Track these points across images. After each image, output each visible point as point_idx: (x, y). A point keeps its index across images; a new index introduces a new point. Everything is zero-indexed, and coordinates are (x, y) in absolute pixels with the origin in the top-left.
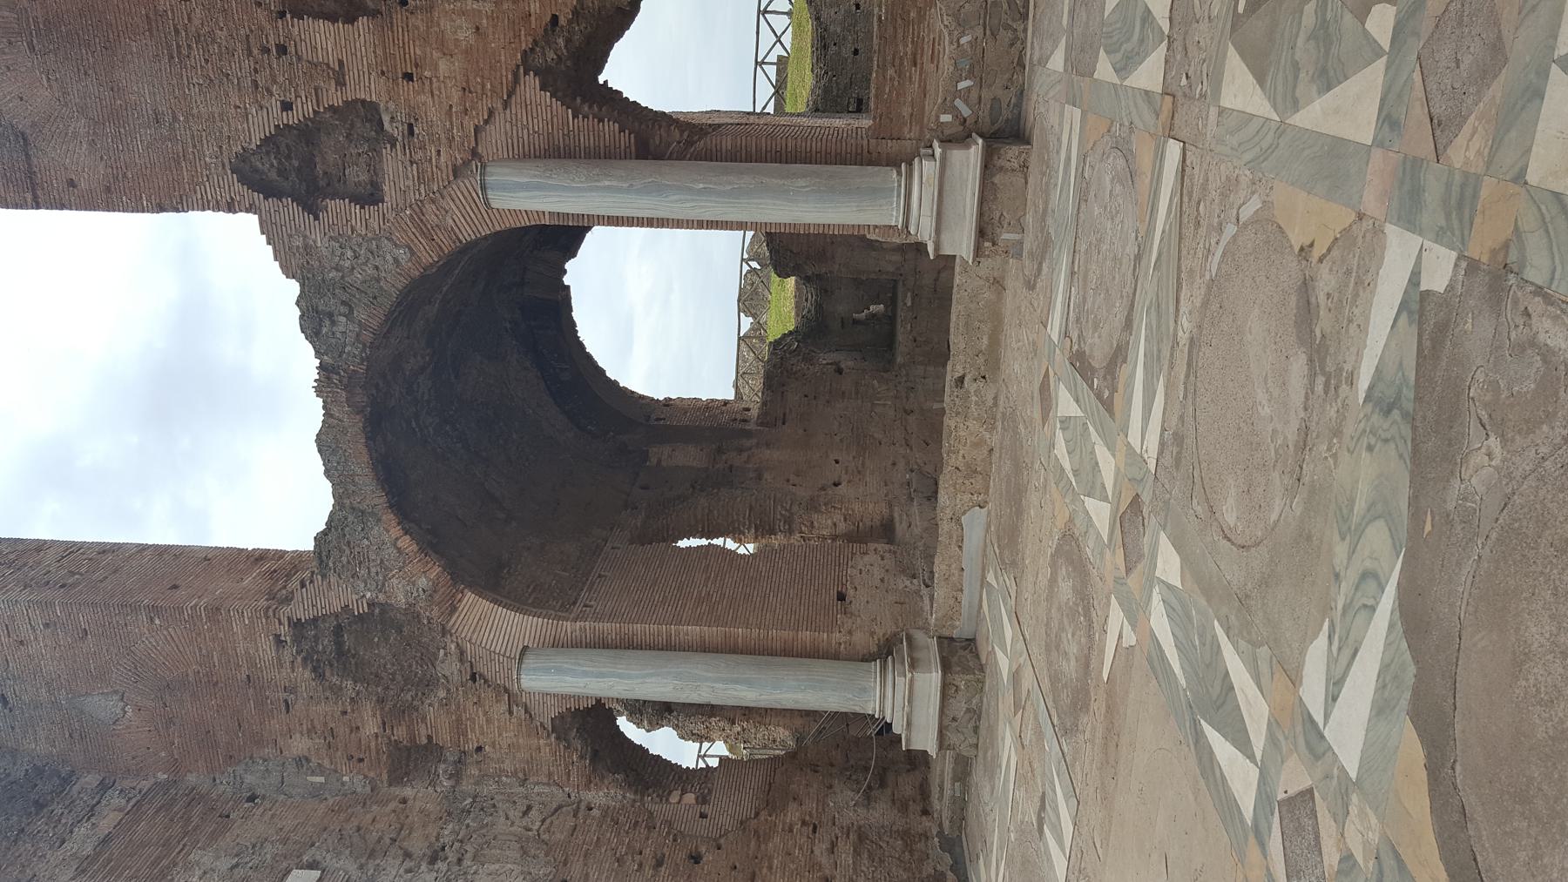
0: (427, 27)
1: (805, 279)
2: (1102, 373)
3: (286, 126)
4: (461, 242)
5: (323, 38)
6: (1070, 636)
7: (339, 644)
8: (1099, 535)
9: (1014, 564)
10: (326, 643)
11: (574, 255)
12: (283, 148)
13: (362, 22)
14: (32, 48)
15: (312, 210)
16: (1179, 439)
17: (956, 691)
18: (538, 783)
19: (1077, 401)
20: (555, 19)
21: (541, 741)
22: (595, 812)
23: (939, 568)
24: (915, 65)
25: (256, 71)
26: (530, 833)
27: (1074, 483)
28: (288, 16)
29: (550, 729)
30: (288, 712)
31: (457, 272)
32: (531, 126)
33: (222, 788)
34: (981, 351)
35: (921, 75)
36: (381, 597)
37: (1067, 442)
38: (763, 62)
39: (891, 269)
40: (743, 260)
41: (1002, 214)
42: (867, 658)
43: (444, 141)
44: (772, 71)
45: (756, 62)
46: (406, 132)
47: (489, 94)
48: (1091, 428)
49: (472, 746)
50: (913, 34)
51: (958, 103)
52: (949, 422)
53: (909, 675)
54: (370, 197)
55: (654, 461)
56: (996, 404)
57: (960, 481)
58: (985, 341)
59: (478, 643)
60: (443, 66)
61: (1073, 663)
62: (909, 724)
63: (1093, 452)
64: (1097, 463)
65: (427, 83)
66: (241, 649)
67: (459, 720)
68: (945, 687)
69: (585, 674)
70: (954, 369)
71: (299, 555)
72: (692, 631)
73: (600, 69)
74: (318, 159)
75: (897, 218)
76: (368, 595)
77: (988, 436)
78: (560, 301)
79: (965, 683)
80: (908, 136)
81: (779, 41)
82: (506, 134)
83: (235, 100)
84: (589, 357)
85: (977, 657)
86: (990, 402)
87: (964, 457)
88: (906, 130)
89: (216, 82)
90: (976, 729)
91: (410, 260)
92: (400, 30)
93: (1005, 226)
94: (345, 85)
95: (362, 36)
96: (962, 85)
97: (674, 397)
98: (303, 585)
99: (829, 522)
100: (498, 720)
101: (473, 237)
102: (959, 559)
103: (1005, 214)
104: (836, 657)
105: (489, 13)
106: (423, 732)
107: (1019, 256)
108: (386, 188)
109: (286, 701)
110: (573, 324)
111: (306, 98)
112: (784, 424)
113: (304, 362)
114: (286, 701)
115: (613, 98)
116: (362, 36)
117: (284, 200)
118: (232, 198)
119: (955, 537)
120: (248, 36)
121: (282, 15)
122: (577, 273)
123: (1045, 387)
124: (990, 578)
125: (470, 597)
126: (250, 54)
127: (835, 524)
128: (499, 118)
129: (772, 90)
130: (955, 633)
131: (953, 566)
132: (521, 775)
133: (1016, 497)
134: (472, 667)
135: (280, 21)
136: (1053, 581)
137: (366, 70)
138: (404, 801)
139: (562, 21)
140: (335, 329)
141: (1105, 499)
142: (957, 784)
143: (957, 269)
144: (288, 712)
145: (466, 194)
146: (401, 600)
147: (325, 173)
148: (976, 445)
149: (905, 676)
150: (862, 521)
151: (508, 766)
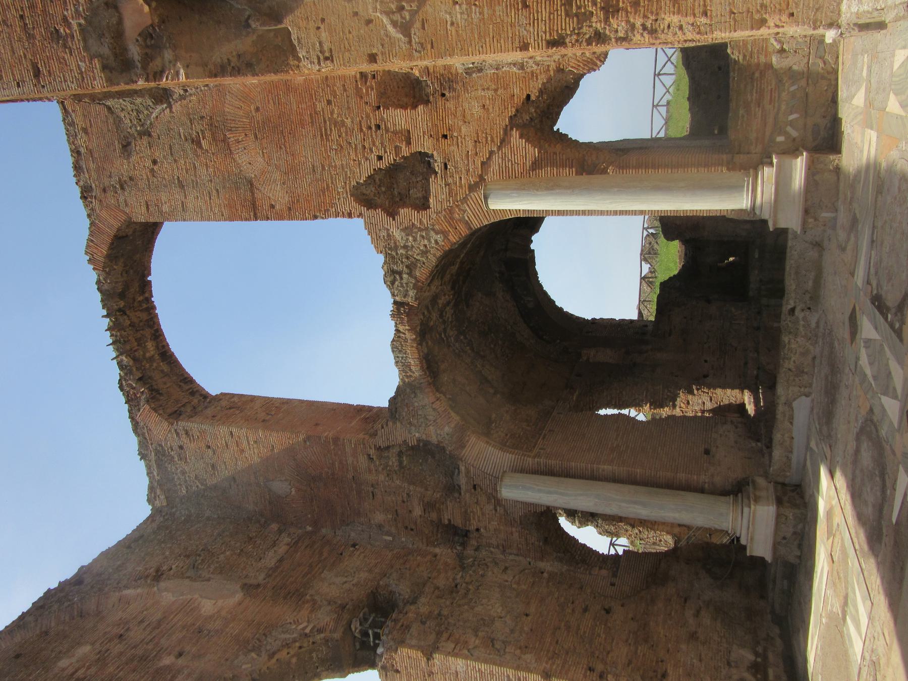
0: (456, 107)
1: (685, 242)
2: (893, 311)
3: (380, 169)
4: (471, 229)
5: (399, 118)
6: (869, 490)
7: (401, 462)
8: (891, 423)
9: (829, 436)
10: (393, 461)
11: (537, 231)
12: (377, 180)
13: (420, 108)
14: (256, 137)
15: (392, 214)
17: (786, 519)
18: (511, 554)
19: (876, 329)
20: (528, 96)
21: (514, 529)
22: (545, 575)
23: (777, 437)
24: (759, 106)
25: (364, 139)
26: (507, 583)
27: (873, 385)
28: (382, 109)
29: (519, 522)
30: (373, 499)
31: (469, 245)
32: (513, 160)
33: (339, 538)
35: (762, 112)
36: (424, 437)
37: (869, 356)
38: (657, 105)
40: (644, 228)
41: (821, 200)
42: (724, 493)
43: (464, 171)
44: (663, 110)
45: (653, 106)
46: (443, 168)
47: (490, 143)
48: (886, 349)
49: (473, 528)
50: (757, 86)
51: (789, 129)
52: (785, 339)
53: (752, 507)
54: (423, 205)
55: (585, 358)
56: (818, 326)
57: (792, 378)
58: (810, 283)
59: (477, 467)
60: (463, 129)
61: (870, 509)
62: (752, 539)
63: (887, 365)
64: (890, 373)
65: (455, 139)
66: (350, 461)
67: (466, 512)
68: (778, 516)
69: (540, 491)
70: (790, 302)
71: (380, 409)
72: (606, 468)
73: (555, 123)
74: (395, 186)
76: (417, 435)
78: (528, 259)
79: (793, 515)
80: (754, 152)
81: (668, 91)
82: (499, 164)
83: (353, 156)
84: (545, 293)
85: (802, 497)
86: (813, 325)
89: (344, 147)
90: (800, 546)
91: (443, 241)
92: (441, 111)
94: (410, 144)
95: (420, 116)
96: (791, 117)
97: (598, 318)
98: (382, 427)
99: (700, 401)
100: (488, 514)
101: (479, 226)
104: (701, 490)
105: (491, 97)
106: (446, 517)
107: (834, 228)
108: (431, 201)
109: (373, 493)
110: (536, 273)
111: (390, 153)
112: (670, 335)
113: (385, 301)
114: (373, 493)
115: (563, 138)
116: (420, 116)
117: (377, 210)
118: (351, 211)
119: (787, 416)
120: (360, 121)
121: (379, 108)
122: (539, 242)
123: (853, 318)
124: (813, 444)
125: (473, 439)
126: (361, 130)
127: (704, 403)
128: (496, 159)
129: (664, 122)
130: (787, 481)
131: (786, 435)
132: (501, 548)
133: (831, 390)
134: (473, 481)
135: (377, 112)
136: (857, 451)
137: (422, 134)
138: (435, 556)
139: (533, 98)
140: (402, 281)
141: (895, 397)
143: (790, 236)
144: (373, 499)
145: (475, 201)
146: (434, 440)
147: (399, 193)
148: (804, 354)
149: (750, 507)
151: (494, 541)
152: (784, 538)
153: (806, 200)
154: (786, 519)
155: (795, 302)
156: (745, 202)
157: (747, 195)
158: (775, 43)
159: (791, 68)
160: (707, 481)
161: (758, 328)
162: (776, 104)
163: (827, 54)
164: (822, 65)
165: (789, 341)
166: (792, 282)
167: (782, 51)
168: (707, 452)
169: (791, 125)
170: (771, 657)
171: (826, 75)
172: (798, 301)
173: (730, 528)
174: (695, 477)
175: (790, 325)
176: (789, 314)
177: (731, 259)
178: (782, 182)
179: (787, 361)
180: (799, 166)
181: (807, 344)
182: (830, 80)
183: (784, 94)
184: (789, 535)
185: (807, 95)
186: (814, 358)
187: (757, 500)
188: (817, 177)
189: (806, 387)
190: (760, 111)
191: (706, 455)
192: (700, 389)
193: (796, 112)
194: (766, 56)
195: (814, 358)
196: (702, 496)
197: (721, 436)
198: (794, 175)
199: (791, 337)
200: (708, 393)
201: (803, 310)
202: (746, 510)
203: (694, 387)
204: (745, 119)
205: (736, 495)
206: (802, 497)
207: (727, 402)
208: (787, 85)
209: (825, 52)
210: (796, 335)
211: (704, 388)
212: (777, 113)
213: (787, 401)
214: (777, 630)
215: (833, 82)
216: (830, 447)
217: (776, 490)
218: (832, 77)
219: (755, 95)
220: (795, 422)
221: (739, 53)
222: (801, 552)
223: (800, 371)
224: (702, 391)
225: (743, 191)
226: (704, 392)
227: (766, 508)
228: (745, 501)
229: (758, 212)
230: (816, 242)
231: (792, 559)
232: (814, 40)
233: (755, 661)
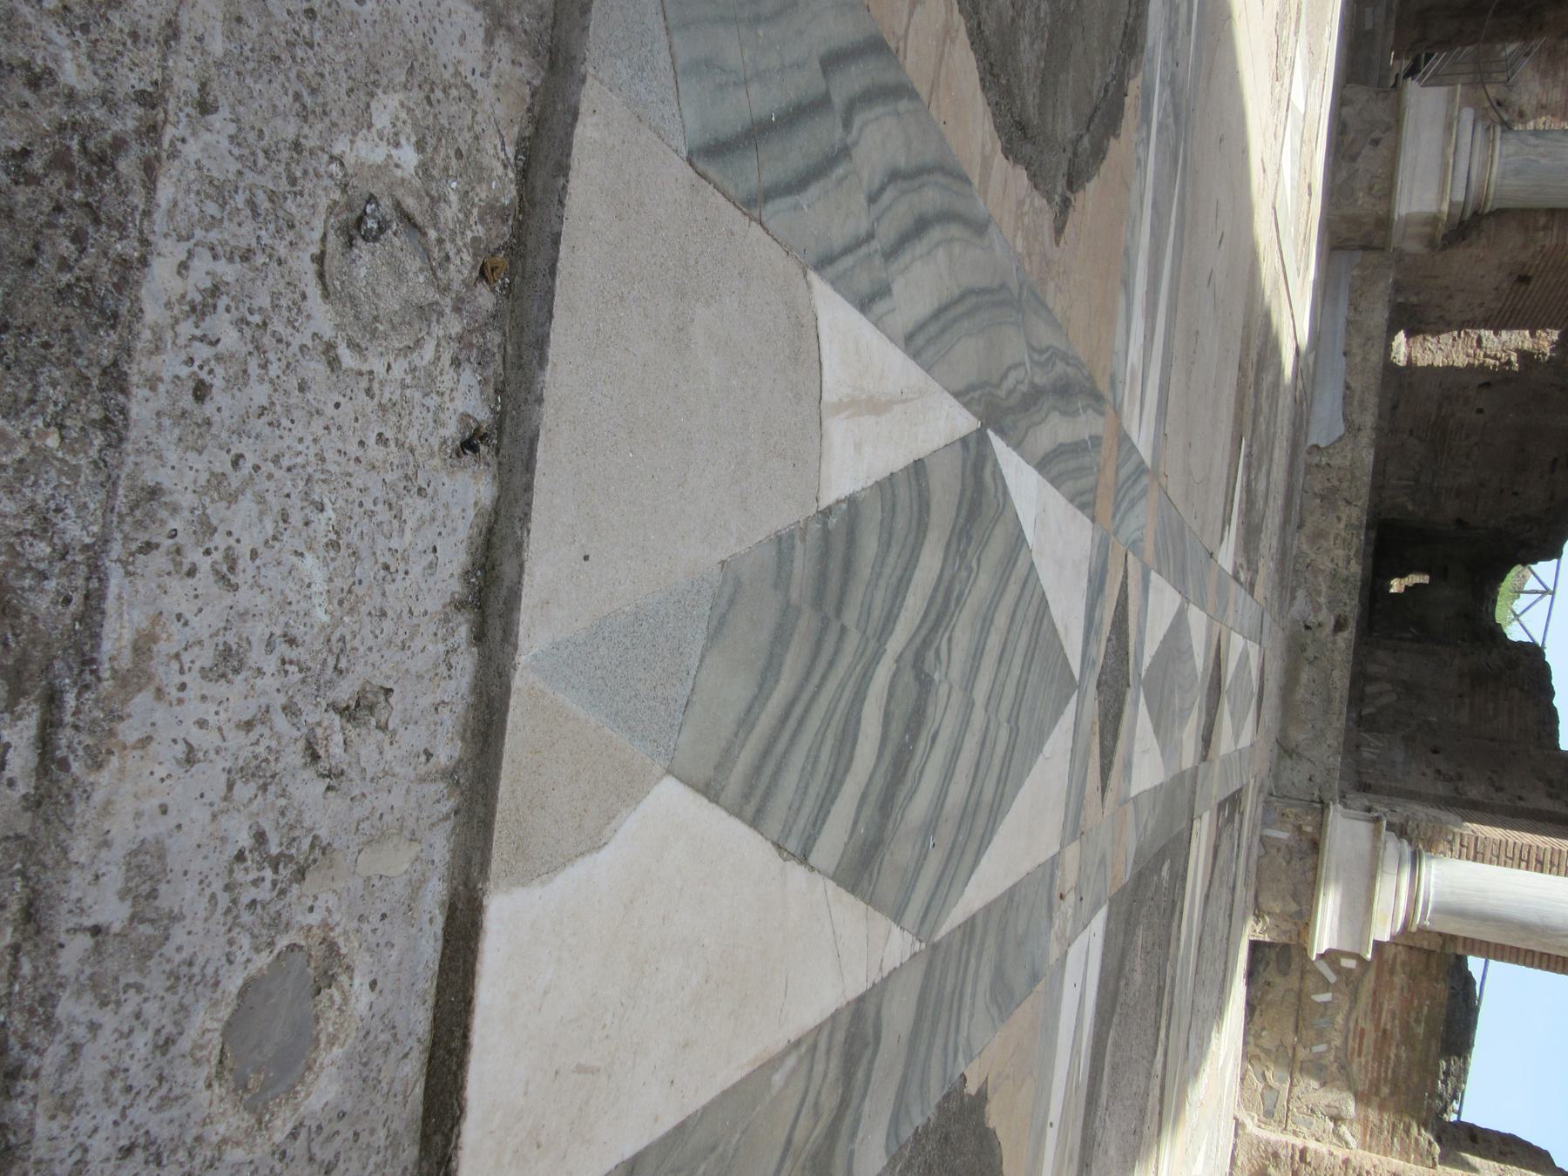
17: (1371, 188)
34: (1310, 663)
39: (1380, 654)
41: (1288, 863)
42: (1499, 213)
50: (1387, 1069)
51: (1332, 978)
52: (1356, 568)
53: (1445, 207)
57: (1345, 485)
58: (1305, 676)
62: (1448, 128)
75: (1429, 872)
77: (1305, 547)
79: (1356, 201)
80: (1400, 948)
86: (1300, 594)
87: (1339, 519)
88: (1403, 956)
93: (1283, 848)
102: (1350, 370)
103: (1284, 864)
112: (1555, 460)
119: (1356, 403)
131: (1358, 359)
148: (1319, 535)
150: (1454, 339)
152: (1376, 142)
153: (1315, 868)
154: (1371, 188)
155: (1334, 642)
157: (1427, 894)
158: (1349, 1137)
159: (1323, 1085)
162: (1352, 1025)
163: (1260, 1090)
164: (1269, 1075)
165: (1349, 562)
166: (1339, 684)
167: (1337, 1119)
168: (1524, 279)
169: (1328, 983)
171: (1262, 1055)
172: (1329, 645)
176: (1346, 619)
180: (1326, 934)
181: (1313, 556)
182: (1256, 1045)
183: (1337, 1042)
184: (1367, 150)
185: (1297, 1030)
186: (1300, 526)
188: (1293, 907)
190: (1383, 1021)
192: (1502, 365)
193: (1319, 1004)
194: (1366, 1118)
195: (1300, 526)
196: (1551, 205)
197: (1481, 305)
198: (1336, 920)
199: (1345, 572)
200: (1486, 356)
201: (1320, 625)
203: (1516, 367)
204: (1413, 1014)
205: (1475, 213)
208: (1332, 1058)
209: (1262, 1095)
210: (1334, 575)
211: (1494, 366)
212: (1351, 1009)
213: (1356, 436)
215: (1251, 1039)
218: (1251, 1048)
219: (1392, 1056)
221: (1417, 1140)
223: (1328, 498)
224: (1499, 359)
226: (1495, 357)
227: (1415, 208)
228: (1457, 212)
229: (1407, 850)
230: (1291, 756)
232: (1280, 1122)
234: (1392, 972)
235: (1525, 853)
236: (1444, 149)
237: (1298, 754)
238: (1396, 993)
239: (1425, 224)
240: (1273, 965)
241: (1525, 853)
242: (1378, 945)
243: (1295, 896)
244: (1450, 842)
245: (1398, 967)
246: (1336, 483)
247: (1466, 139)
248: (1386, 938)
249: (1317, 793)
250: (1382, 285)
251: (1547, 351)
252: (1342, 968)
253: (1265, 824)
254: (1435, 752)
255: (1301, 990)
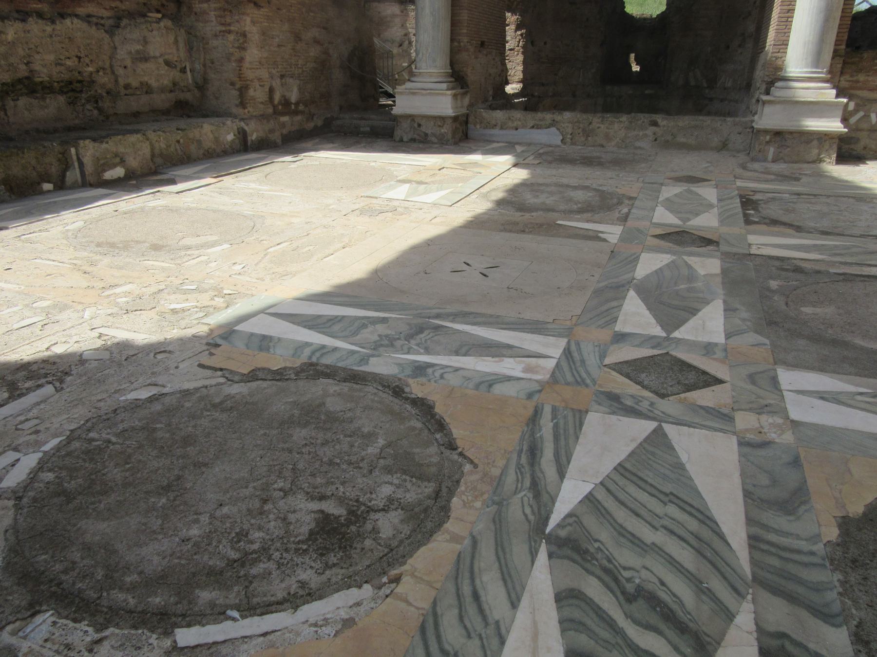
16: (798, 270)
17: (440, 126)
41: (788, 147)
42: (452, 64)
51: (861, 114)
52: (624, 118)
53: (449, 92)
56: (636, 148)
57: (581, 126)
58: (683, 140)
68: (442, 118)
75: (794, 72)
77: (613, 143)
86: (638, 144)
87: (599, 128)
88: (847, 77)
90: (413, 140)
93: (779, 150)
102: (524, 127)
103: (789, 149)
104: (452, 40)
119: (541, 123)
130: (471, 126)
131: (519, 123)
142: (368, 129)
148: (608, 137)
152: (419, 125)
153: (791, 133)
154: (440, 126)
156: (798, 70)
160: (462, 44)
161: (574, 96)
169: (865, 116)
170: (299, 118)
173: (421, 71)
174: (465, 31)
175: (640, 122)
176: (651, 121)
177: (636, 68)
178: (817, 108)
179: (599, 120)
180: (834, 125)
181: (618, 139)
184: (423, 129)
186: (602, 146)
187: (455, 96)
188: (815, 143)
189: (571, 139)
191: (480, 43)
195: (602, 146)
196: (449, 40)
197: (494, 59)
198: (821, 117)
200: (518, 46)
201: (654, 134)
202: (444, 86)
203: (524, 31)
205: (452, 76)
206: (460, 140)
207: (509, 66)
210: (627, 128)
213: (557, 122)
214: (320, 123)
216: (540, 163)
217: (463, 115)
220: (535, 131)
222: (407, 142)
223: (587, 133)
225: (813, 67)
226: (519, 42)
227: (450, 106)
228: (451, 85)
229: (779, 84)
231: (398, 133)
233: (291, 103)
234: (858, 82)
235: (783, 19)
236: (423, 95)
237: (726, 141)
238: (870, 79)
239: (457, 99)
240: (852, 146)
241: (783, 19)
242: (837, 96)
243: (808, 142)
244: (777, 59)
245: (855, 78)
246: (581, 130)
247: (419, 85)
248: (834, 92)
249: (748, 130)
250: (484, 114)
251: (516, 17)
252: (854, 110)
253: (765, 160)
254: (728, 47)
255: (870, 130)
